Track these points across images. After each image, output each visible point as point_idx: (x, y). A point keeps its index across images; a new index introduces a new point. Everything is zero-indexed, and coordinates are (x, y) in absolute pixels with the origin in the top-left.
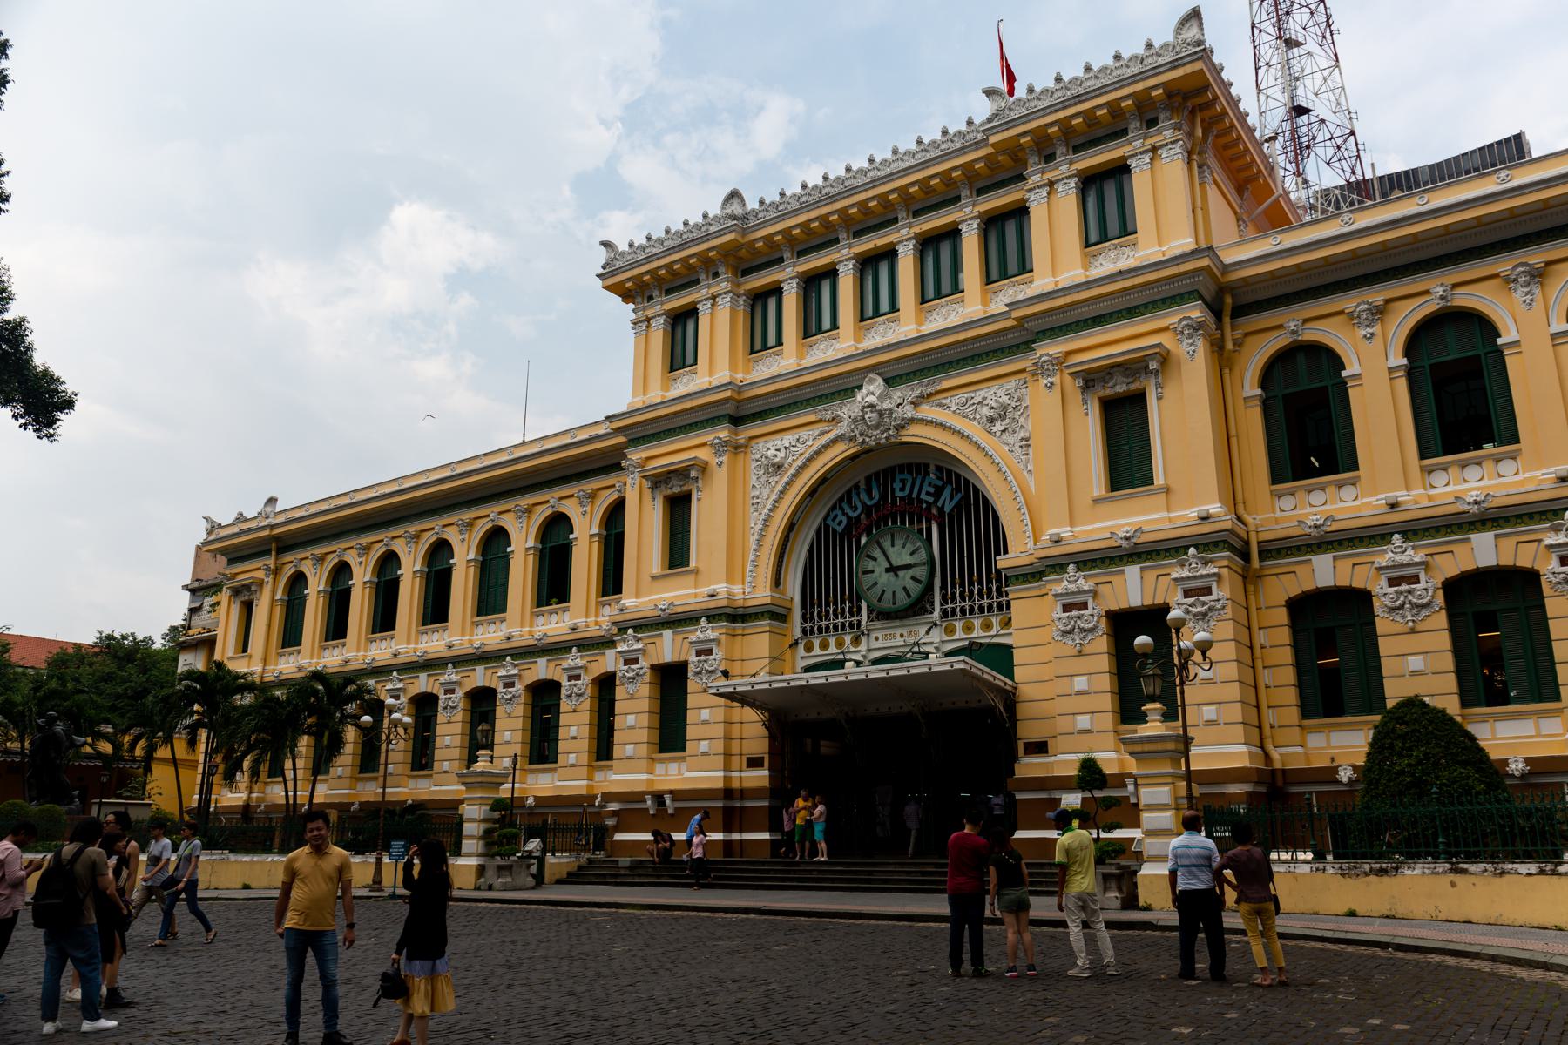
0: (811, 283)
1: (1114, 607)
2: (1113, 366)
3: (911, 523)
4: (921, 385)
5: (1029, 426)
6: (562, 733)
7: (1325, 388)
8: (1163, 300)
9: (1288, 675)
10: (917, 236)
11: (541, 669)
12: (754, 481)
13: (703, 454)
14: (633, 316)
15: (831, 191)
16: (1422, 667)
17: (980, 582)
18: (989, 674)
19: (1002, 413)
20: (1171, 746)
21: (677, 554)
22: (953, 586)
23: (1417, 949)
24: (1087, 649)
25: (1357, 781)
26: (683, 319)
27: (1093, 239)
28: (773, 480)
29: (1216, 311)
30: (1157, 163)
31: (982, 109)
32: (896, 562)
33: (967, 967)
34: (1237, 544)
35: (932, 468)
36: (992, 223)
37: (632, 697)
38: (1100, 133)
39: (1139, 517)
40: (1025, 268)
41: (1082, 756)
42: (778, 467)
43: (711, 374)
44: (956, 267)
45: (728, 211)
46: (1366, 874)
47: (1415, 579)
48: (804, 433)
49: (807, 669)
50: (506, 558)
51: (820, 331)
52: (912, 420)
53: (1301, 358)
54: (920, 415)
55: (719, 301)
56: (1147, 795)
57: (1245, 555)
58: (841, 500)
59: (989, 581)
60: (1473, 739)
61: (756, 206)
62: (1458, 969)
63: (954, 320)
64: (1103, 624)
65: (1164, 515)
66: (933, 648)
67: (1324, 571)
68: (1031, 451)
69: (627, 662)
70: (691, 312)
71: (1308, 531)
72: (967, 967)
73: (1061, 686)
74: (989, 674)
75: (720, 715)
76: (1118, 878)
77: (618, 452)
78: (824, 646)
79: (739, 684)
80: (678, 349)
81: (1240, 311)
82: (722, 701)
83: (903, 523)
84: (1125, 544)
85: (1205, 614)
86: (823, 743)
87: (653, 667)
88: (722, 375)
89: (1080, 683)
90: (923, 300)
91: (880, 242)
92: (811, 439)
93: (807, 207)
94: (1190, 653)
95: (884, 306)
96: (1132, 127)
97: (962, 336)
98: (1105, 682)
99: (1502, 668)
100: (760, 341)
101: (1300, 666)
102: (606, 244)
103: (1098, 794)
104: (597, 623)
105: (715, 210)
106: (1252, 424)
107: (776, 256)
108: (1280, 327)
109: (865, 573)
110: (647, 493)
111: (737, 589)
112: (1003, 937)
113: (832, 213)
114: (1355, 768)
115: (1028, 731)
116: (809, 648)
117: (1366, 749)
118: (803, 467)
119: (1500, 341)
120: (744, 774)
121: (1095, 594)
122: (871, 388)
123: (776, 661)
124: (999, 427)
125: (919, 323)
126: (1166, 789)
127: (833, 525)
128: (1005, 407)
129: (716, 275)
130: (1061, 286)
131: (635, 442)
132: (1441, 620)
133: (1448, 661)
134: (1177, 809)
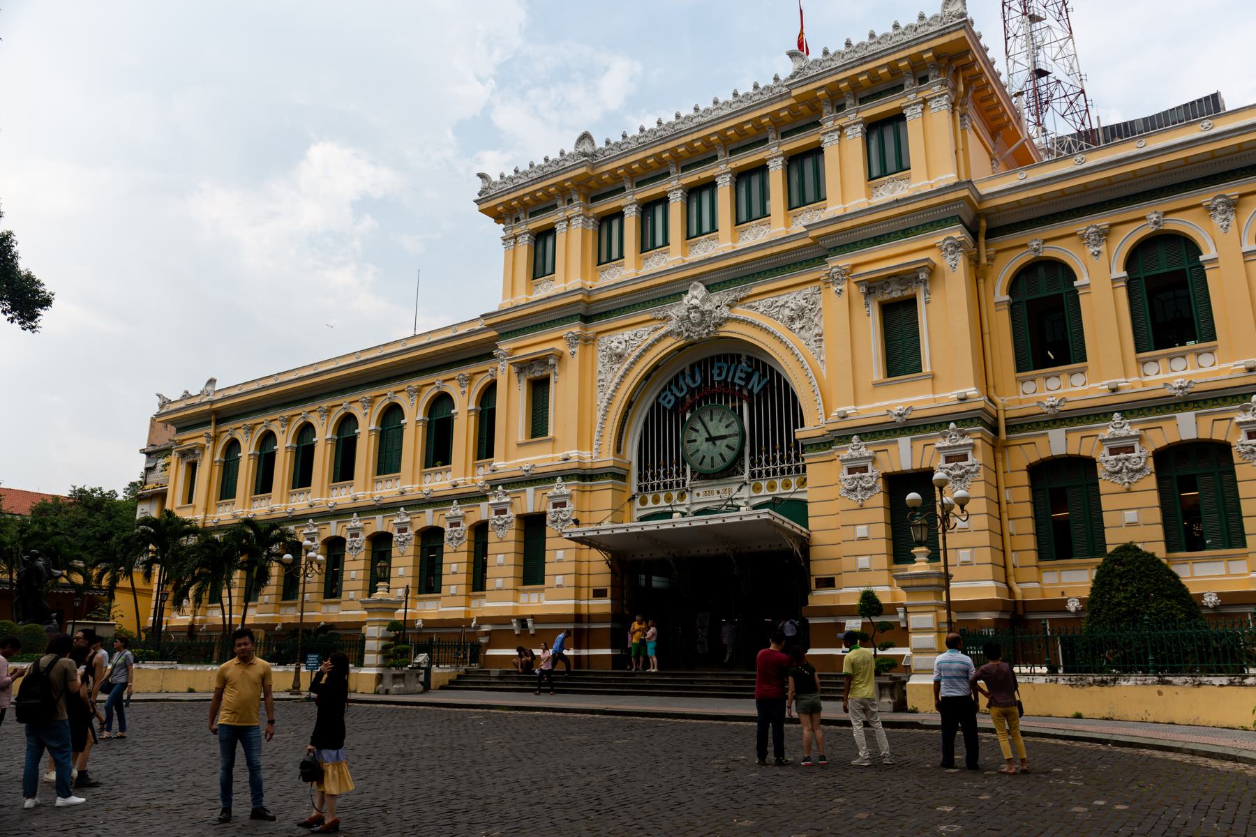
0: (647, 208)
1: (889, 470)
2: (890, 276)
3: (727, 402)
4: (735, 291)
5: (822, 324)
6: (445, 569)
7: (1061, 295)
8: (931, 224)
9: (1029, 526)
10: (733, 171)
11: (429, 518)
12: (600, 367)
13: (560, 346)
14: (503, 234)
15: (664, 134)
16: (1135, 520)
17: (782, 450)
18: (789, 524)
19: (800, 314)
20: (934, 581)
21: (538, 426)
22: (760, 453)
23: (1130, 745)
24: (867, 504)
25: (1083, 610)
26: (543, 236)
27: (875, 174)
29: (974, 234)
30: (927, 113)
31: (786, 68)
32: (714, 433)
33: (771, 757)
34: (989, 420)
35: (744, 358)
36: (794, 160)
37: (501, 541)
38: (881, 88)
39: (910, 398)
40: (820, 197)
41: (862, 589)
42: (620, 356)
43: (566, 281)
44: (765, 196)
45: (581, 150)
46: (1090, 685)
47: (1131, 449)
48: (641, 329)
49: (642, 519)
50: (401, 428)
51: (654, 247)
52: (728, 319)
53: (1041, 271)
54: (734, 315)
55: (573, 222)
56: (915, 620)
57: (995, 430)
58: (670, 383)
59: (789, 449)
60: (1176, 577)
61: (603, 146)
62: (1166, 760)
63: (762, 239)
64: (880, 484)
65: (931, 396)
66: (743, 502)
67: (1058, 443)
68: (823, 344)
69: (497, 513)
70: (550, 231)
71: (1045, 410)
72: (771, 757)
73: (846, 533)
74: (789, 524)
75: (572, 555)
76: (891, 687)
77: (491, 344)
78: (656, 500)
79: (588, 530)
80: (540, 261)
81: (992, 233)
82: (573, 544)
83: (720, 402)
84: (898, 419)
85: (962, 476)
86: (654, 578)
87: (518, 517)
88: (575, 282)
89: (862, 531)
90: (738, 222)
91: (703, 175)
92: (646, 334)
93: (644, 146)
94: (951, 507)
95: (706, 227)
96: (907, 83)
97: (768, 252)
98: (881, 530)
99: (1199, 521)
100: (605, 255)
101: (1038, 518)
102: (482, 176)
103: (876, 620)
104: (473, 481)
105: (570, 148)
106: (1001, 326)
107: (620, 186)
108: (1025, 245)
110: (514, 377)
111: (586, 454)
112: (799, 733)
113: (665, 151)
114: (1081, 600)
115: (819, 569)
116: (644, 502)
117: (1090, 585)
118: (639, 357)
119: (1201, 258)
120: (591, 602)
121: (873, 460)
122: (695, 293)
123: (617, 511)
124: (797, 325)
125: (735, 241)
126: (930, 616)
127: (664, 403)
128: (803, 309)
129: (570, 201)
130: (848, 211)
131: (505, 335)
132: (1152, 482)
133: (1157, 515)
134: (939, 632)
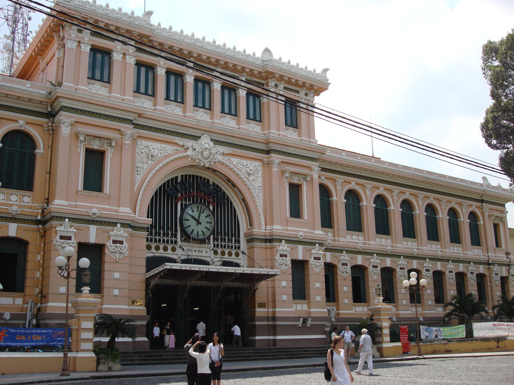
28: (150, 162)
35: (211, 183)
52: (219, 162)
84: (301, 238)
109: (211, 223)
116: (149, 248)
124: (251, 178)
